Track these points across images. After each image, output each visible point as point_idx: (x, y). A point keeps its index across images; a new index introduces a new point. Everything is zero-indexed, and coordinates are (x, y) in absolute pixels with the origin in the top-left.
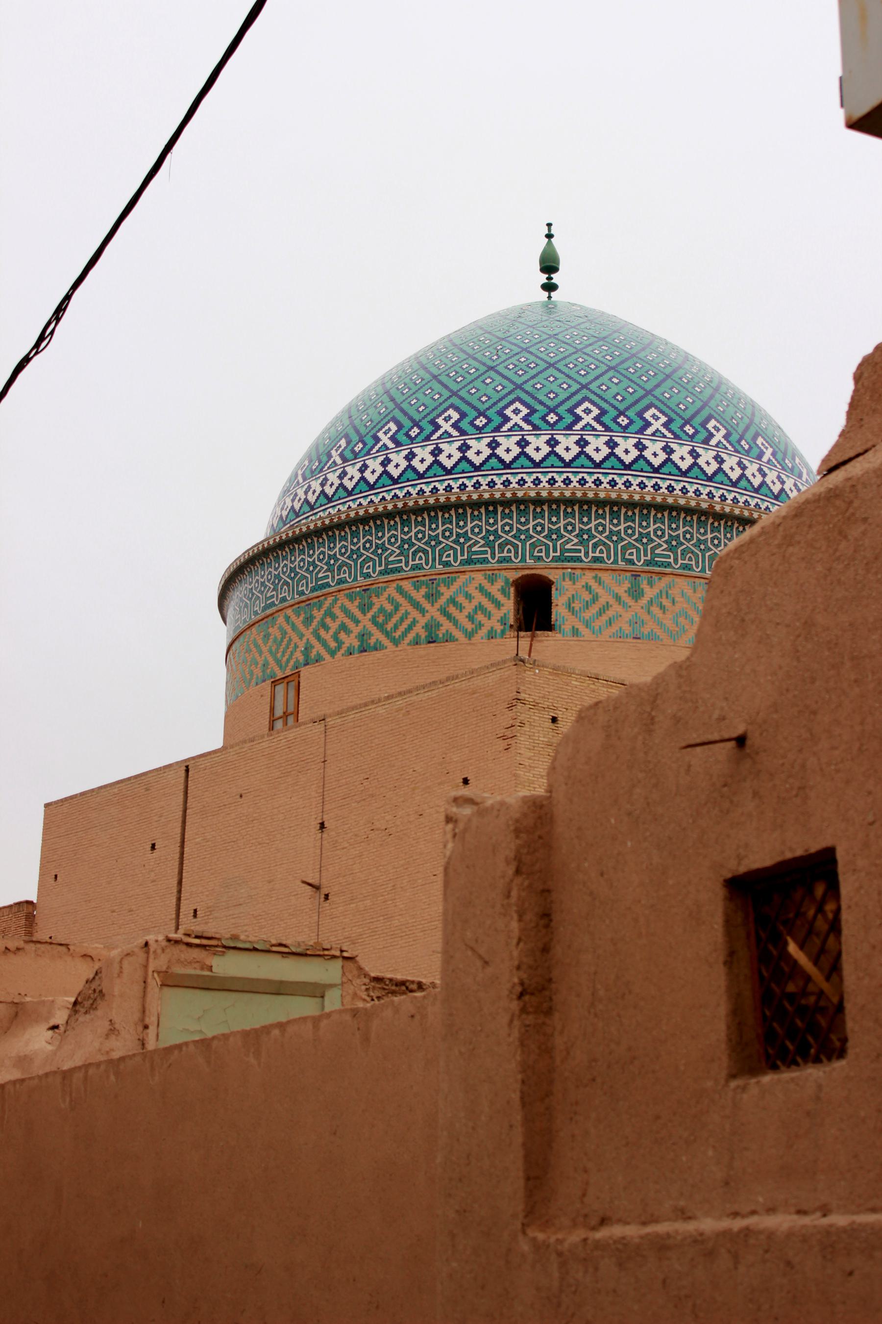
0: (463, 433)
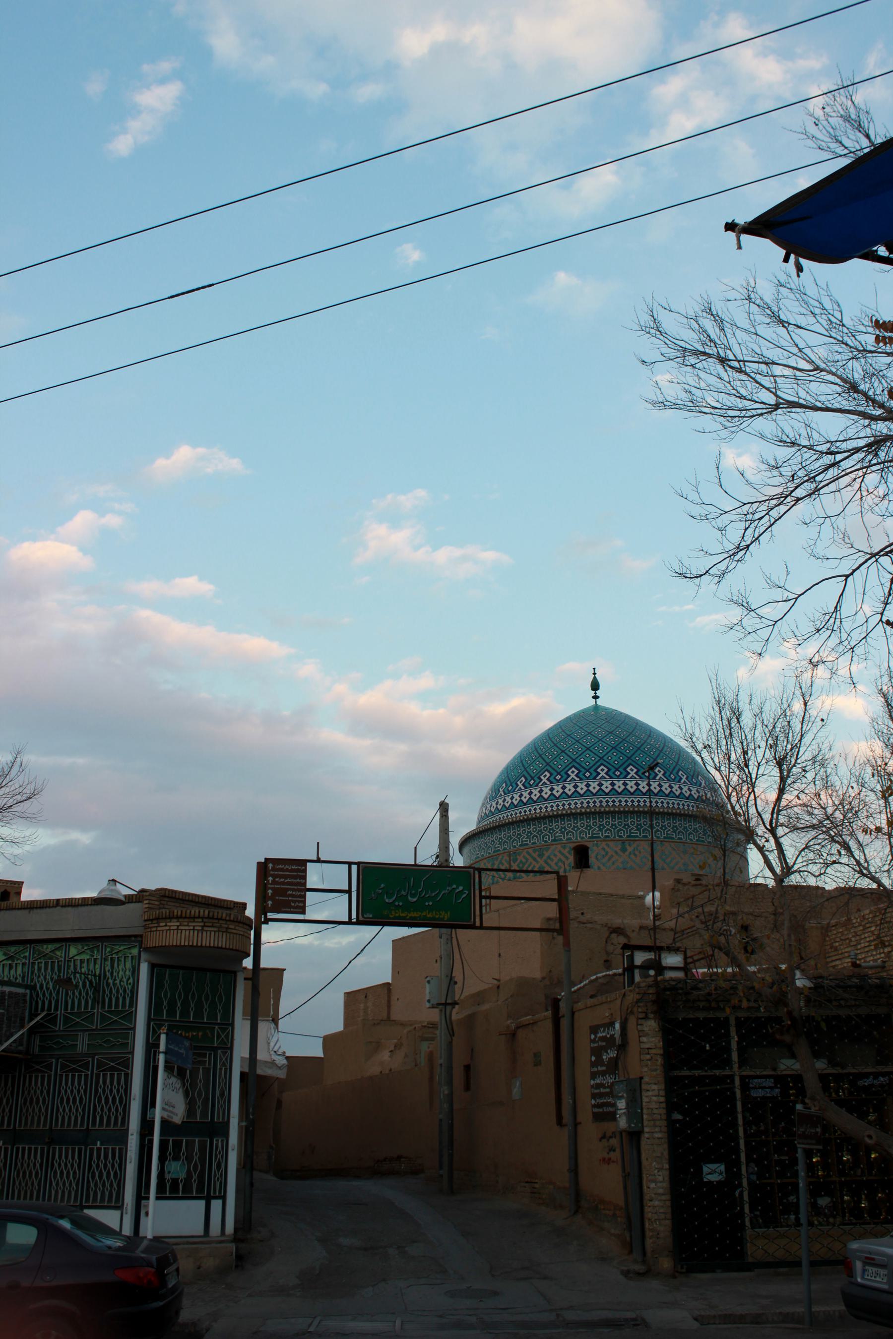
0: (551, 783)
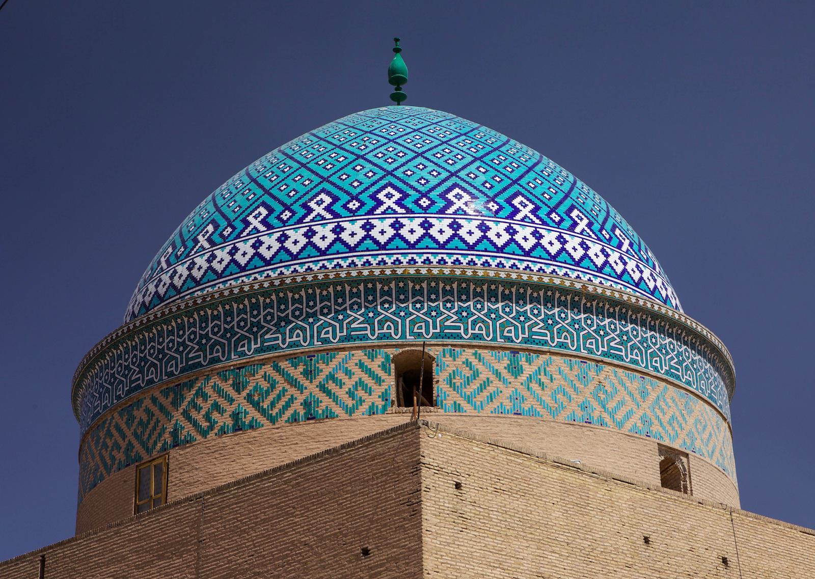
0: (336, 215)
